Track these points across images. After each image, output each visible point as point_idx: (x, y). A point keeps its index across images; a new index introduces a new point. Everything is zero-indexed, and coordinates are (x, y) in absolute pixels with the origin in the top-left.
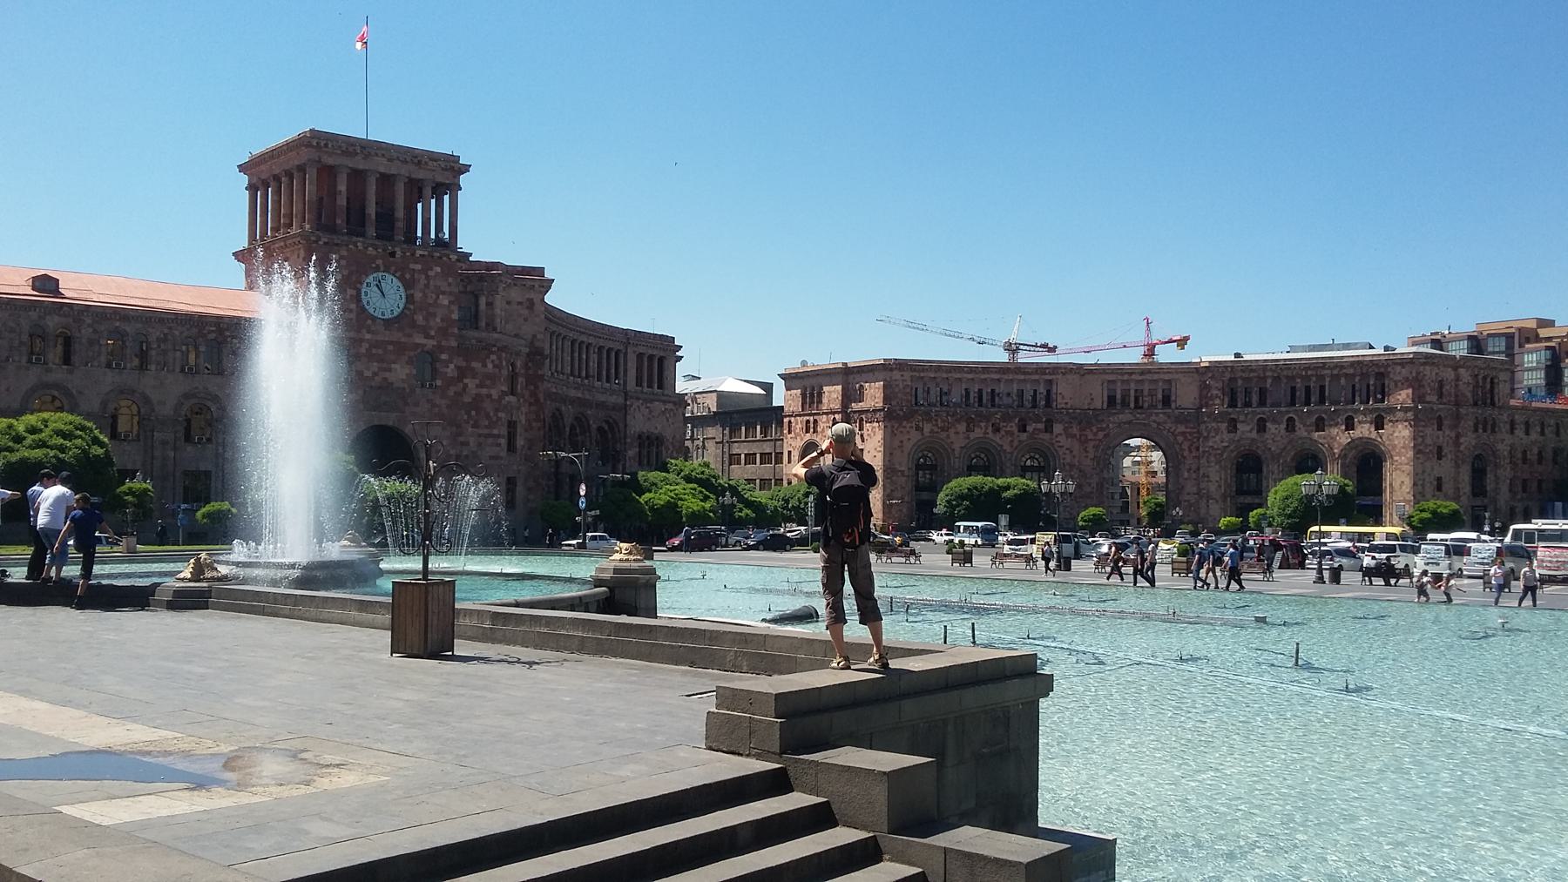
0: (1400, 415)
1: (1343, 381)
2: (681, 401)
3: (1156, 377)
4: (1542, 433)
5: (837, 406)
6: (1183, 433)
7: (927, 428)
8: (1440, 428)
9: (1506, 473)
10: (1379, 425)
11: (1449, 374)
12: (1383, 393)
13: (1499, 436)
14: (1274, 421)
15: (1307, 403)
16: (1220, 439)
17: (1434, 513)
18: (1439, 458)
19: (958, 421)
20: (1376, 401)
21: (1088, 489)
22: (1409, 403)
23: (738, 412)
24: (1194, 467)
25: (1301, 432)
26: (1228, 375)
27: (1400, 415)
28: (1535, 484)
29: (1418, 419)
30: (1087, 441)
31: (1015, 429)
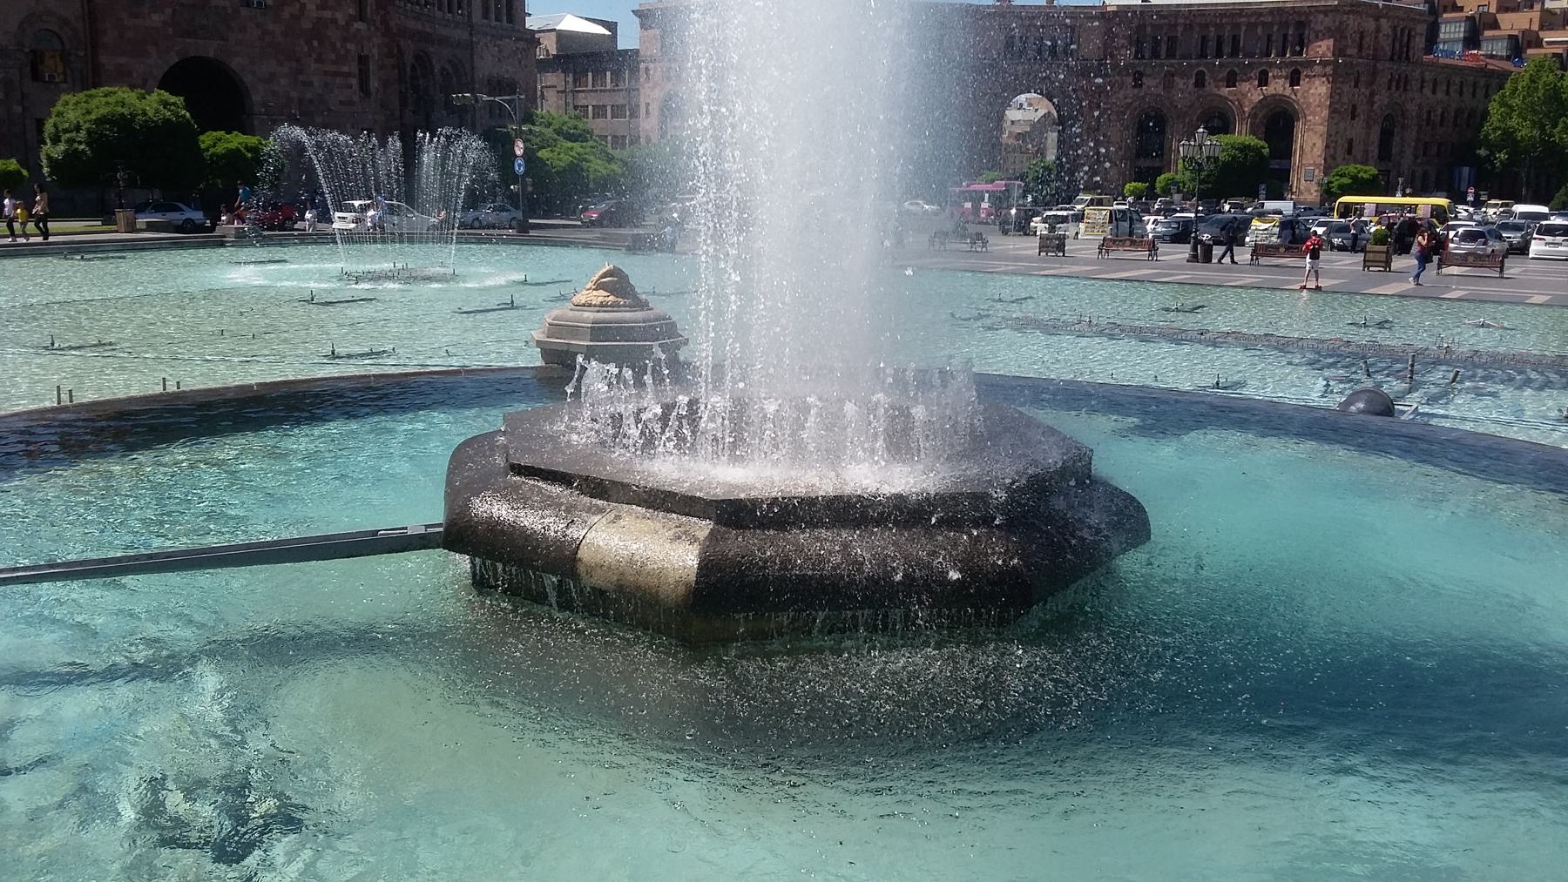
0: (1318, 69)
1: (1259, 31)
2: (532, 39)
4: (1448, 93)
8: (1356, 86)
9: (1411, 134)
10: (1294, 80)
11: (1370, 25)
12: (1302, 43)
14: (1183, 75)
15: (1219, 55)
17: (1354, 178)
18: (1353, 118)
20: (1294, 53)
22: (1329, 57)
23: (585, 55)
25: (1211, 87)
27: (1318, 69)
28: (1435, 149)
29: (1339, 74)
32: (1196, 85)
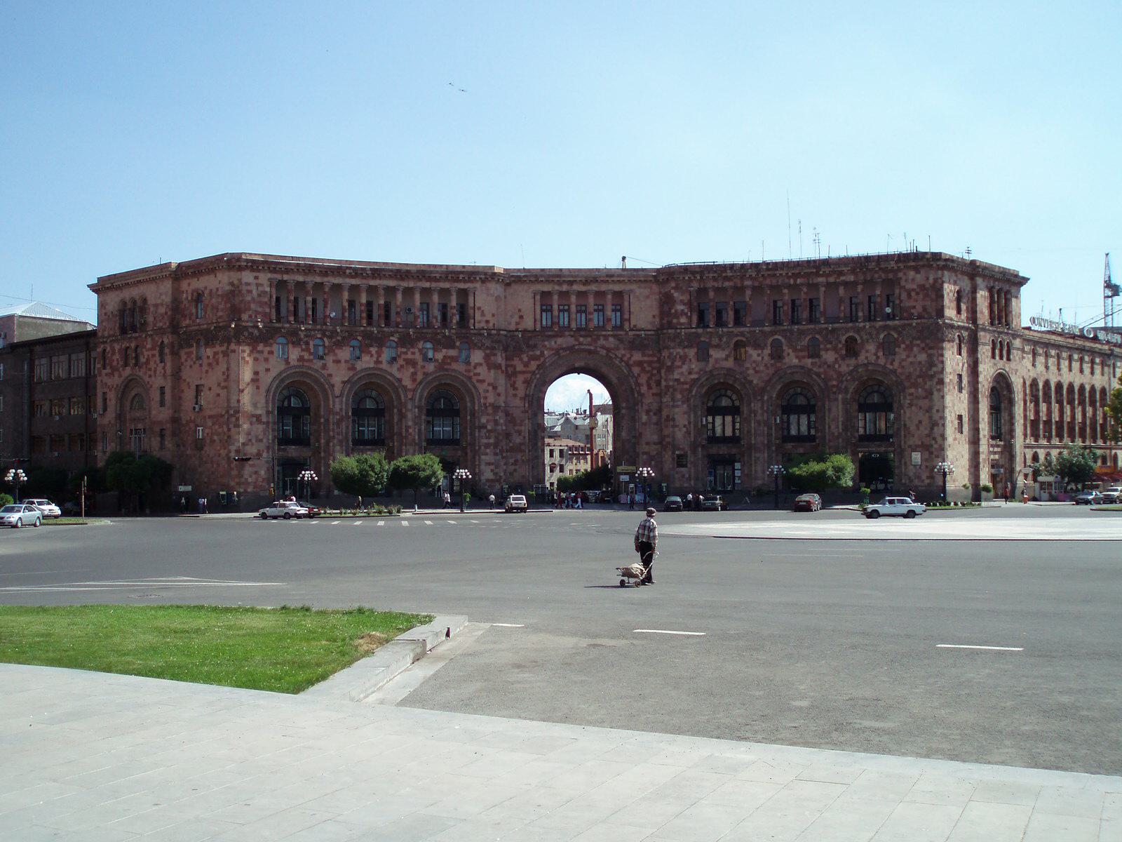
1: (841, 291)
3: (604, 287)
5: (164, 323)
6: (640, 364)
7: (294, 354)
10: (888, 347)
13: (1013, 365)
14: (757, 346)
16: (687, 368)
19: (339, 345)
21: (518, 440)
24: (655, 407)
25: (791, 359)
26: (695, 285)
30: (515, 373)
31: (418, 357)
32: (771, 356)
